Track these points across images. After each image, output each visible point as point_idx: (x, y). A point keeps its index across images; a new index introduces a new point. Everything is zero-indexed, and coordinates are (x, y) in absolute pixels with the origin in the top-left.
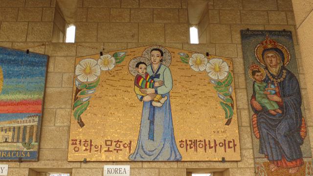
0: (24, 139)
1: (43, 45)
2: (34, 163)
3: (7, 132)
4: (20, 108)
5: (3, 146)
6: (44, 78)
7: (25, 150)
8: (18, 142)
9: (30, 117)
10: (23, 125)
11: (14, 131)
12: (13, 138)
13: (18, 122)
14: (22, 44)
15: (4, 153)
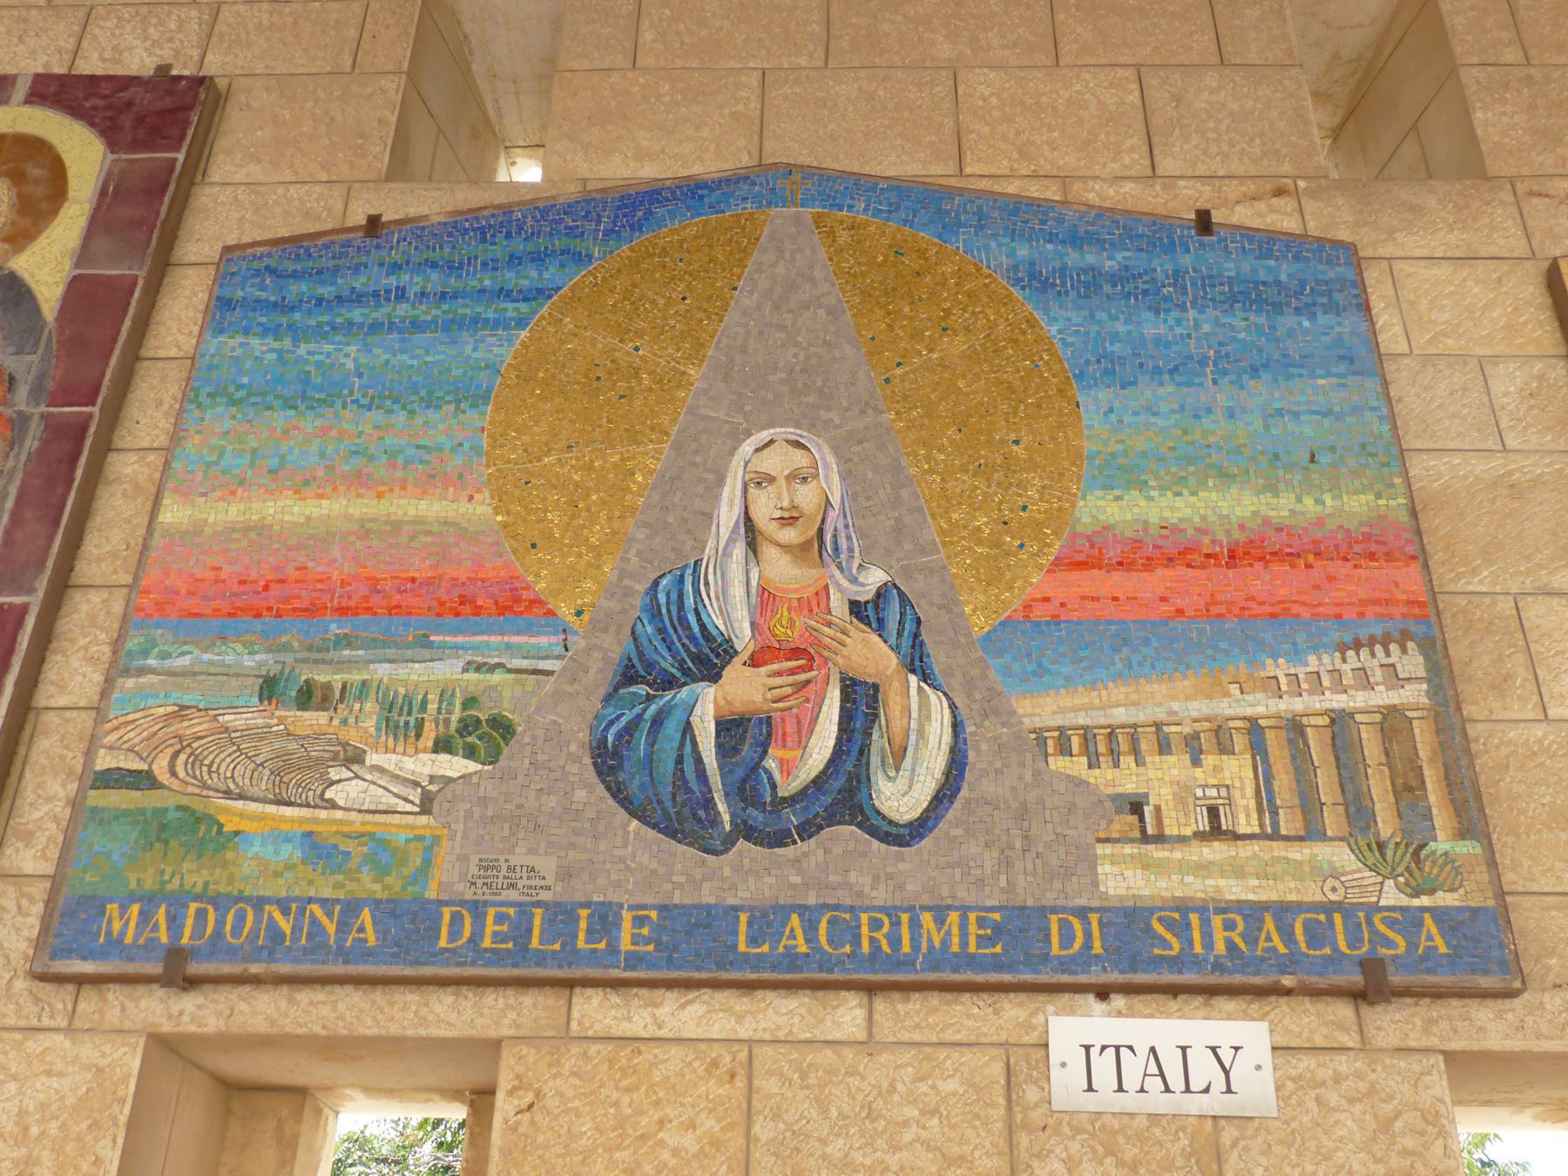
0: (1359, 813)
1: (1279, 192)
2: (1483, 1013)
3: (1209, 760)
4: (1259, 581)
5: (1204, 868)
6: (1372, 384)
7: (1392, 896)
8: (1313, 832)
9: (1357, 646)
10: (1316, 703)
11: (1258, 748)
12: (1266, 802)
13: (1272, 686)
14: (1128, 187)
15: (1229, 926)
